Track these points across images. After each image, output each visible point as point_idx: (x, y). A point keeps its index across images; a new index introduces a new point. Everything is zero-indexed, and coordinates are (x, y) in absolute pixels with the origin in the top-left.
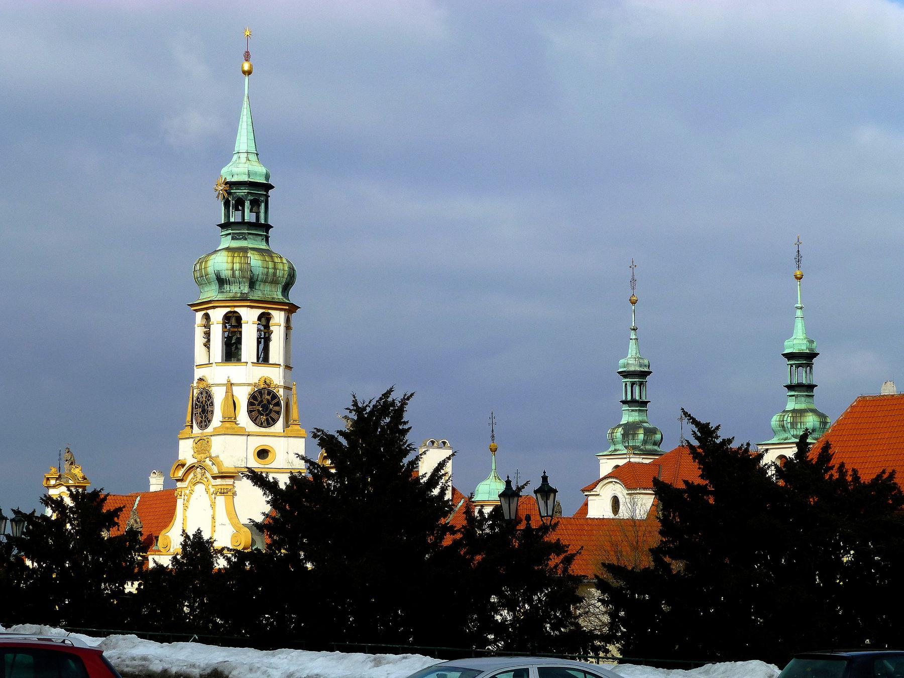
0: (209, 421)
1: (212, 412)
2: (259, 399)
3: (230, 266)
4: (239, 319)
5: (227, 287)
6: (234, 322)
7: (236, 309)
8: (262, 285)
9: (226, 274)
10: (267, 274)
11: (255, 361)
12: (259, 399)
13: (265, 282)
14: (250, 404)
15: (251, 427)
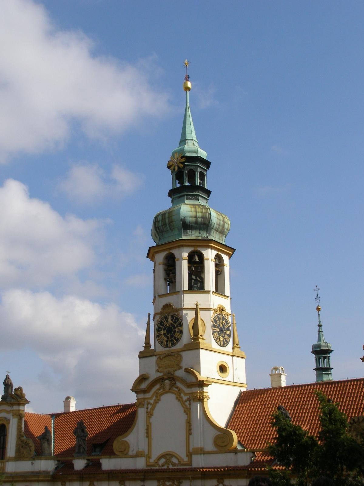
0: (178, 340)
1: (181, 332)
2: (218, 323)
3: (194, 214)
4: (201, 257)
5: (190, 232)
6: (197, 259)
7: (199, 249)
8: (215, 232)
9: (189, 220)
10: (219, 225)
11: (215, 291)
12: (218, 323)
13: (217, 231)
14: (214, 326)
15: (215, 345)
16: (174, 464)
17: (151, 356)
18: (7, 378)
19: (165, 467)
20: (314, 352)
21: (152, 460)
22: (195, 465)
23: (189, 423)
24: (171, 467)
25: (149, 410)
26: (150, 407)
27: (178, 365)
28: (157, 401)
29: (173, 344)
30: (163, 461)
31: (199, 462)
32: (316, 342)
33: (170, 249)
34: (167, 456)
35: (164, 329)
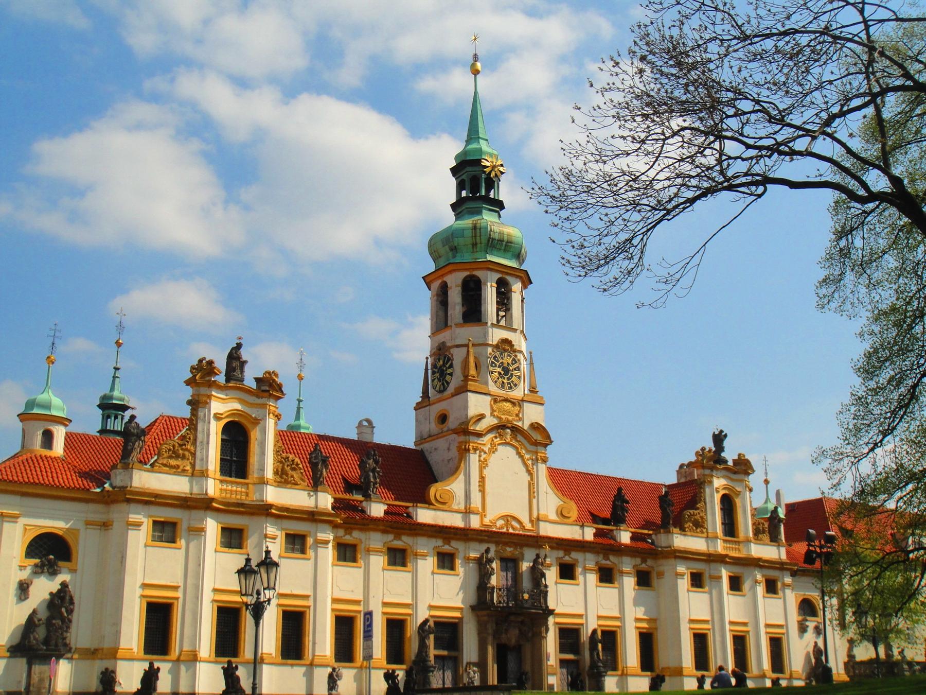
0: (516, 385)
16: (513, 528)
17: (485, 394)
18: (239, 346)
19: (504, 530)
20: (100, 406)
21: (487, 521)
22: (543, 532)
23: (530, 485)
24: (511, 531)
25: (482, 459)
26: (484, 456)
27: (517, 415)
28: (493, 450)
29: (511, 388)
30: (501, 523)
31: (547, 530)
32: (107, 392)
33: (507, 274)
34: (508, 518)
35: (499, 367)
